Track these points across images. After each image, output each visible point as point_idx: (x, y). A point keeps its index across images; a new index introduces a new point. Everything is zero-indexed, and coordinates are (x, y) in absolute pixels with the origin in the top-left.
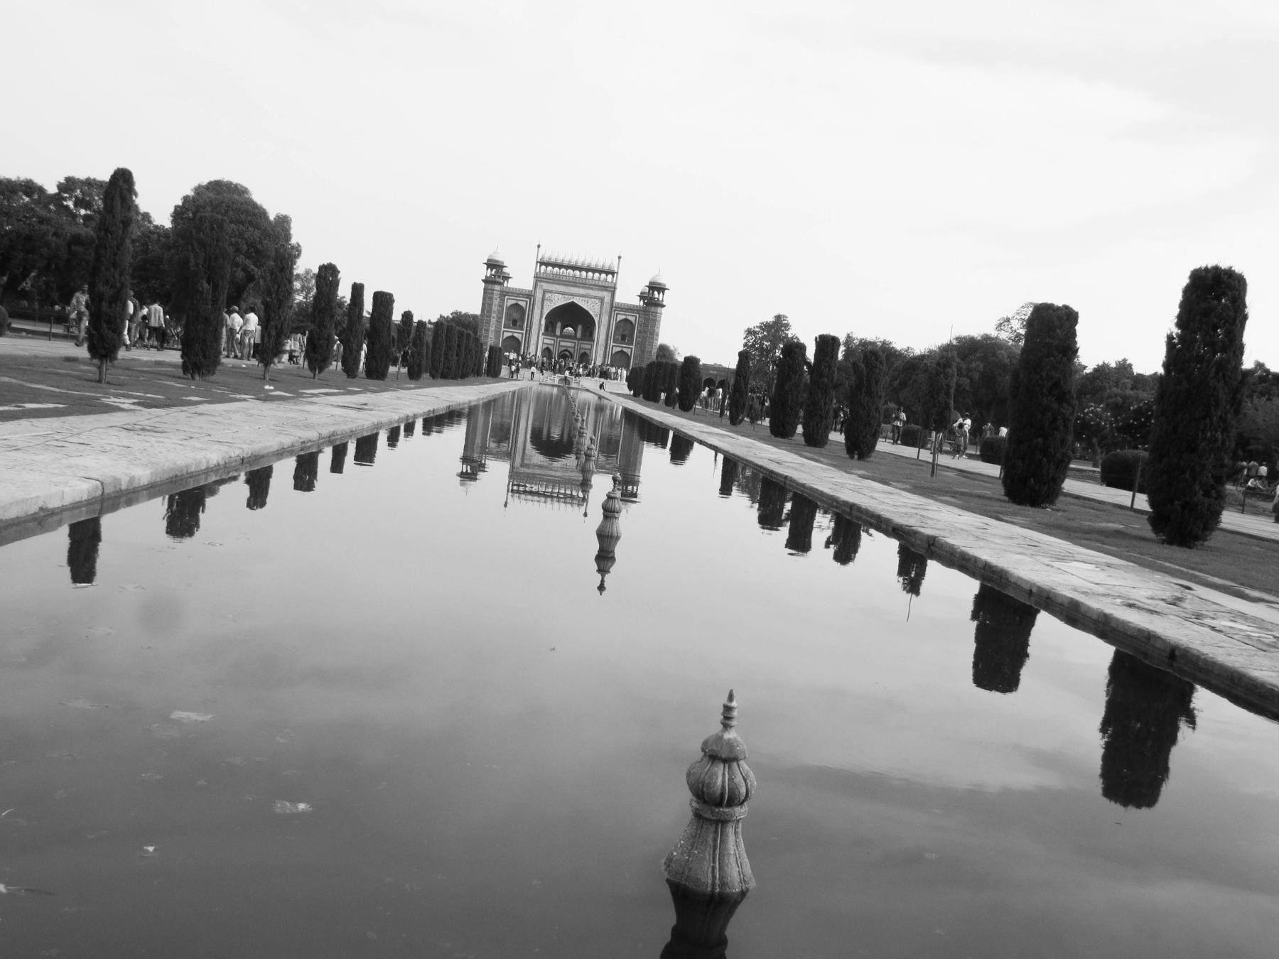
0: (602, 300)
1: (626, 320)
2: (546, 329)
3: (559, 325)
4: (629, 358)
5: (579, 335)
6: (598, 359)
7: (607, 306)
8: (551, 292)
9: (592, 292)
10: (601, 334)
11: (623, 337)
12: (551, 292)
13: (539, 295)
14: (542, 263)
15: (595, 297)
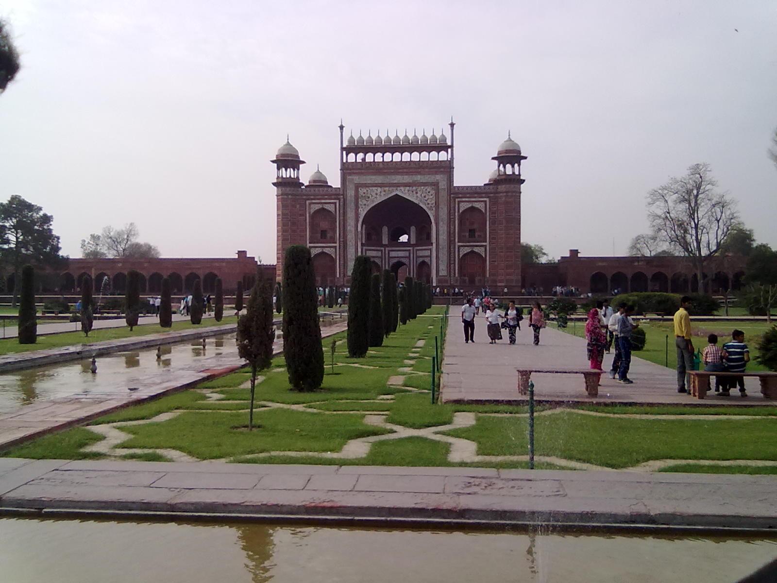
0: (435, 185)
1: (472, 208)
2: (369, 236)
3: (385, 230)
4: (485, 260)
5: (413, 241)
6: (440, 269)
7: (444, 195)
8: (365, 186)
9: (419, 178)
10: (439, 232)
11: (472, 232)
12: (365, 186)
13: (351, 193)
14: (348, 150)
15: (425, 184)
